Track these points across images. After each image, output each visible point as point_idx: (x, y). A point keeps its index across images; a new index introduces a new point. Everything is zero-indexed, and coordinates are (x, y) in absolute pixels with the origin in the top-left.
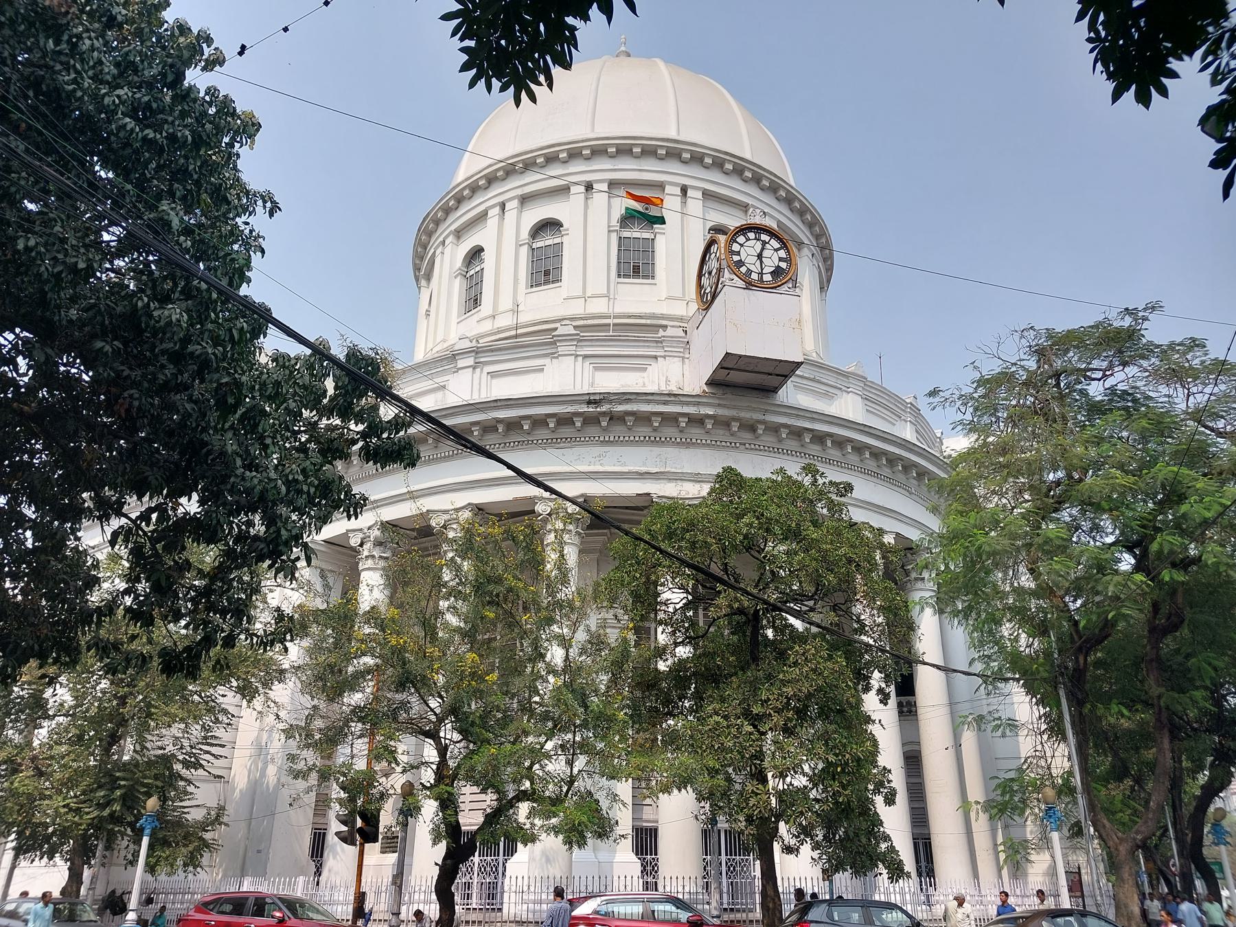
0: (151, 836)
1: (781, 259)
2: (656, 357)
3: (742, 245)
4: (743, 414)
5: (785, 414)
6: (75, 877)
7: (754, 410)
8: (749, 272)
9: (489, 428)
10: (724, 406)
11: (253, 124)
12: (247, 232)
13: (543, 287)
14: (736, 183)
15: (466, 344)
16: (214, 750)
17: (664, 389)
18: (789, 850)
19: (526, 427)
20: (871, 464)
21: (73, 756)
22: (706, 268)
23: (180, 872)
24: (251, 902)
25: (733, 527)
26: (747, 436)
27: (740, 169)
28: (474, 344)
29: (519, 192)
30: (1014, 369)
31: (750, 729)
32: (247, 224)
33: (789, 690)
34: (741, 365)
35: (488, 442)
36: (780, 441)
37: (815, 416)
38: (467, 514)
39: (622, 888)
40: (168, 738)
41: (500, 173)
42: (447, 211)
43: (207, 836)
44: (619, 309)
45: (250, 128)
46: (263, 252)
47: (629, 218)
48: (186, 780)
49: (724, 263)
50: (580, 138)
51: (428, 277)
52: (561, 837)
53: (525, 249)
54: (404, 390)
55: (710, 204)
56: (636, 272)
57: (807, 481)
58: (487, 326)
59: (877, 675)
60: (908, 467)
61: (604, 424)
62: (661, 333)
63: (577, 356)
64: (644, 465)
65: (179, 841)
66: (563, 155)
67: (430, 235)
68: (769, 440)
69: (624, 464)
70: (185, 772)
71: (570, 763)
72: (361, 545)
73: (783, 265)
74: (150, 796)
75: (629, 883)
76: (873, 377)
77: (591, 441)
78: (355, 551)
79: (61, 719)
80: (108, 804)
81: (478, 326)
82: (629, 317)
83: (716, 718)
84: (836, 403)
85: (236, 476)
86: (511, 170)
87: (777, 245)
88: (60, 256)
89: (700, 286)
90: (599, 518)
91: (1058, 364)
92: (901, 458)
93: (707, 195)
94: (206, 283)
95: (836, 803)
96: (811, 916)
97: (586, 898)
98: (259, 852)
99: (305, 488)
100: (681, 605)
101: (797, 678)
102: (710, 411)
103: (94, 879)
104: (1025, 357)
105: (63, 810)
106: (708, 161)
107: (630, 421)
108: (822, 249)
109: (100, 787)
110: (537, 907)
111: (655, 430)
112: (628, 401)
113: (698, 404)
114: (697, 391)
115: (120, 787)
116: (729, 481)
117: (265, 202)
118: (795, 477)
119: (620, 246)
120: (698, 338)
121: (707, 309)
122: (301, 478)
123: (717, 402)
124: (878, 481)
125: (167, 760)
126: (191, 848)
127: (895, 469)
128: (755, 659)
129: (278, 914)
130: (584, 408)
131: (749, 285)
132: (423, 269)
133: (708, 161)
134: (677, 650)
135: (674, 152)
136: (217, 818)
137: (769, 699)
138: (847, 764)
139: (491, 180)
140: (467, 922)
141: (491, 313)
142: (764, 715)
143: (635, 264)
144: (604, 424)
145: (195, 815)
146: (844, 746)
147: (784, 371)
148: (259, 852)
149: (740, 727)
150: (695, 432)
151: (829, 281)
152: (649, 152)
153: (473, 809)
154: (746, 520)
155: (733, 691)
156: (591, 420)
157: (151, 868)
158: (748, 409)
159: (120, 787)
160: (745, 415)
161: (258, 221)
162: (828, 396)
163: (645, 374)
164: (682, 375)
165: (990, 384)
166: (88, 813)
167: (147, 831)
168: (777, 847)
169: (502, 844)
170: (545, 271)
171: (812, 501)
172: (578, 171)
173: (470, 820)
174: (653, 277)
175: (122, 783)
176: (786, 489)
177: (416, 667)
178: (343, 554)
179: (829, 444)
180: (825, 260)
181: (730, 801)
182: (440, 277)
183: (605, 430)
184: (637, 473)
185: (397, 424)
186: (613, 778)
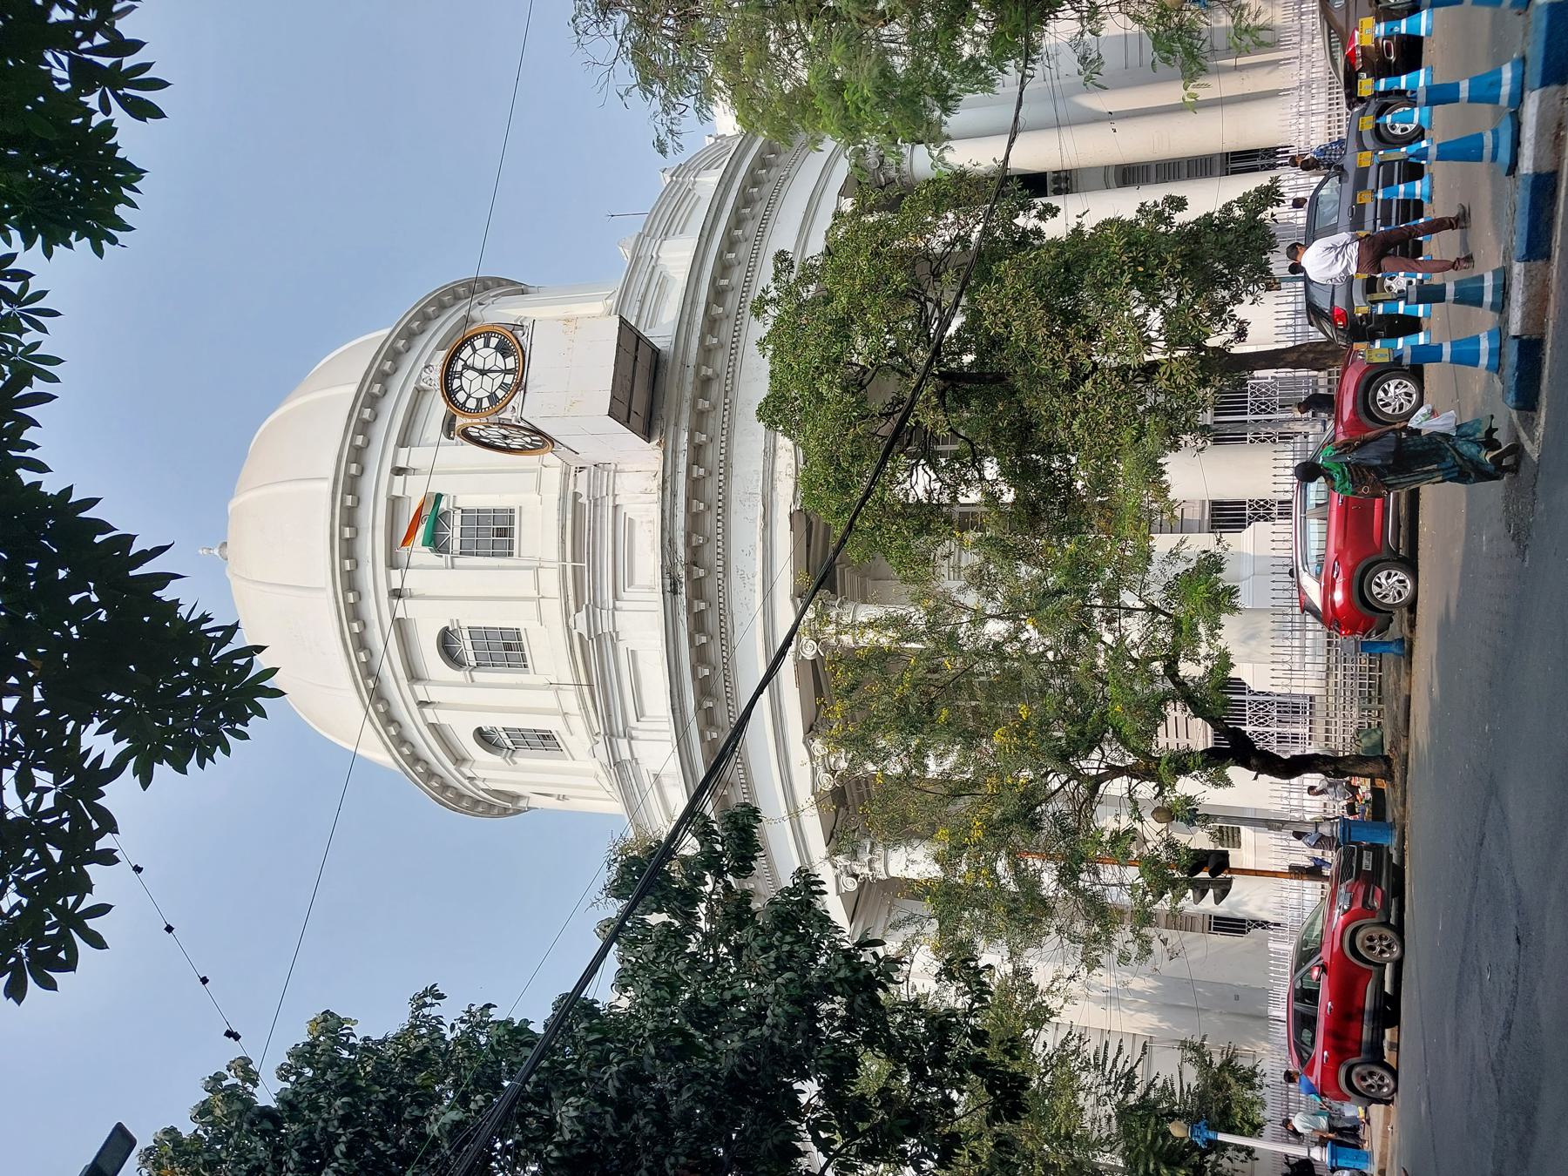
0: (1217, 1131)
1: (487, 345)
2: (615, 507)
3: (469, 396)
4: (688, 394)
5: (687, 340)
7: (682, 380)
8: (503, 386)
9: (708, 719)
11: (325, 1020)
12: (463, 1027)
13: (527, 652)
14: (388, 405)
15: (601, 748)
16: (1112, 1055)
17: (656, 496)
18: (1241, 334)
19: (707, 672)
20: (751, 228)
22: (499, 443)
24: (1299, 1006)
26: (715, 389)
27: (370, 399)
28: (600, 739)
29: (404, 683)
30: (628, 44)
31: (1089, 383)
32: (453, 1027)
33: (1041, 333)
35: (727, 720)
36: (721, 345)
37: (689, 301)
38: (817, 745)
39: (1288, 545)
40: (1095, 1110)
41: (380, 707)
42: (430, 774)
43: (1217, 1061)
44: (554, 554)
45: (330, 1025)
46: (489, 1006)
47: (436, 543)
48: (1149, 1089)
49: (493, 419)
50: (333, 605)
51: (516, 797)
53: (479, 676)
54: (662, 826)
55: (415, 437)
56: (505, 532)
58: (578, 723)
59: (1020, 221)
60: (753, 180)
62: (584, 500)
63: (615, 608)
64: (754, 520)
65: (1223, 1097)
66: (356, 627)
67: (461, 796)
68: (720, 360)
69: (753, 547)
70: (1139, 1091)
71: (1130, 611)
72: (856, 876)
73: (494, 342)
74: (1166, 1134)
75: (1281, 537)
76: (638, 225)
77: (724, 590)
78: (864, 884)
81: (578, 735)
82: (564, 541)
84: (671, 272)
85: (772, 1035)
86: (377, 695)
89: (522, 450)
90: (822, 578)
92: (743, 189)
93: (404, 442)
94: (529, 1076)
95: (1183, 272)
96: (1324, 305)
98: (1237, 998)
99: (786, 948)
101: (1025, 324)
102: (685, 436)
104: (611, 27)
106: (359, 440)
107: (697, 540)
110: (1309, 651)
111: (709, 508)
112: (672, 542)
113: (675, 451)
114: (659, 453)
115: (1157, 1170)
116: (775, 412)
117: (425, 1005)
118: (768, 328)
119: (472, 554)
120: (590, 454)
121: (552, 441)
122: (773, 953)
124: (772, 219)
125: (1124, 1112)
126: (1231, 1081)
128: (1000, 378)
129: (1316, 973)
130: (682, 598)
131: (520, 386)
132: (504, 805)
133: (359, 440)
134: (989, 477)
135: (350, 485)
136: (1196, 1051)
138: (1134, 259)
139: (389, 719)
140: (1327, 739)
141: (560, 718)
142: (1072, 365)
143: (495, 533)
144: (701, 573)
145: (1192, 1076)
146: (1111, 262)
147: (631, 341)
148: (1237, 998)
149: (1087, 397)
150: (712, 455)
151: (513, 283)
152: (349, 517)
153: (1187, 732)
154: (824, 390)
155: (1042, 403)
157: (1256, 1129)
159: (1157, 1170)
160: (688, 392)
163: (637, 521)
164: (637, 472)
165: (648, 75)
167: (1211, 1135)
168: (1238, 349)
170: (506, 649)
171: (800, 305)
172: (377, 610)
173: (1200, 736)
174: (512, 511)
175: (1152, 1166)
176: (783, 341)
177: (1012, 805)
178: (865, 903)
179: (724, 282)
181: (1180, 408)
182: (514, 782)
183: (709, 572)
185: (705, 833)
186: (1149, 558)
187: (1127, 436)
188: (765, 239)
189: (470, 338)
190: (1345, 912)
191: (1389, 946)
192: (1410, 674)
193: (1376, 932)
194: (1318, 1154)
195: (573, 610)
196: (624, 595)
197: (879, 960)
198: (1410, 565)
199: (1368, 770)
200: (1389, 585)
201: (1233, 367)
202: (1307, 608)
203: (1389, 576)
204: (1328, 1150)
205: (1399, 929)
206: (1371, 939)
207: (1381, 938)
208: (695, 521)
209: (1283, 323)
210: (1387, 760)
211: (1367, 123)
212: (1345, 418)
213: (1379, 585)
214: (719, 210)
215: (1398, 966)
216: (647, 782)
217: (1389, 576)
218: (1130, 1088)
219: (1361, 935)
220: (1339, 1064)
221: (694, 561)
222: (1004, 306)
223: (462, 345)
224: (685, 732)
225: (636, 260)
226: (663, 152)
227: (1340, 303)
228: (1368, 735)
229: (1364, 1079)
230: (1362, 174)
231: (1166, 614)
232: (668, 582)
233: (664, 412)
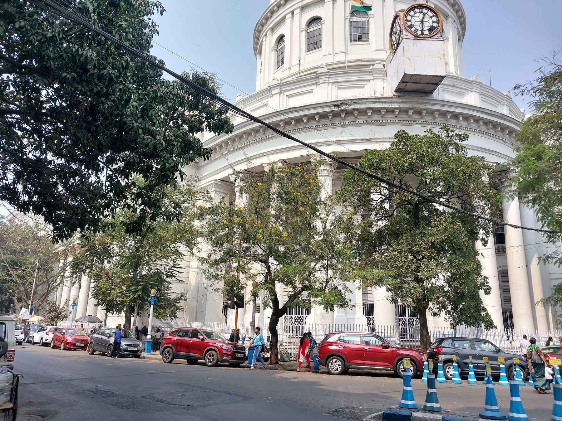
0: (154, 304)
1: (434, 22)
2: (369, 80)
3: (412, 16)
6: (128, 320)
7: (420, 103)
9: (287, 123)
12: (150, 23)
15: (276, 82)
17: (373, 96)
18: (435, 314)
19: (305, 121)
20: (484, 128)
21: (121, 272)
22: (394, 31)
23: (169, 318)
24: (190, 332)
25: (402, 159)
26: (417, 117)
28: (279, 82)
29: (300, 4)
31: (412, 257)
34: (413, 79)
35: (288, 130)
36: (435, 119)
37: (453, 104)
38: (279, 165)
39: (355, 330)
40: (161, 264)
42: (267, 19)
43: (178, 305)
44: (350, 58)
46: (158, 33)
48: (168, 282)
49: (403, 27)
51: (260, 53)
52: (322, 306)
53: (304, 33)
56: (360, 38)
57: (444, 135)
58: (287, 73)
60: (504, 128)
63: (329, 83)
64: (364, 135)
65: (167, 307)
67: (260, 32)
70: (167, 279)
71: (327, 273)
72: (235, 181)
73: (435, 25)
74: (152, 288)
75: (358, 327)
76: (486, 82)
77: (336, 125)
79: (117, 257)
80: (137, 291)
81: (282, 74)
82: (356, 61)
83: (394, 253)
85: (140, 138)
87: (430, 14)
88: (39, 31)
89: (391, 41)
90: (340, 162)
92: (500, 124)
94: (104, 36)
96: (444, 344)
97: (335, 333)
98: (202, 312)
99: (175, 143)
100: (379, 201)
101: (435, 233)
102: (397, 105)
103: (135, 321)
105: (119, 294)
107: (356, 113)
108: (459, 18)
109: (134, 285)
111: (369, 117)
112: (355, 103)
113: (391, 102)
114: (391, 95)
115: (141, 285)
116: (402, 137)
117: (157, 8)
118: (437, 133)
119: (351, 26)
120: (390, 68)
121: (394, 52)
122: (173, 138)
123: (401, 100)
124: (487, 137)
125: (158, 274)
126: (171, 309)
127: (497, 130)
128: (416, 225)
129: (202, 337)
130: (332, 109)
131: (416, 37)
132: (258, 50)
136: (181, 298)
137: (422, 244)
138: (462, 274)
140: (286, 343)
141: (288, 66)
142: (419, 251)
143: (359, 35)
144: (343, 116)
145: (173, 296)
146: (461, 265)
148: (202, 312)
149: (406, 258)
150: (390, 117)
151: (463, 35)
154: (410, 155)
155: (404, 240)
156: (336, 115)
158: (417, 103)
159: (141, 285)
160: (415, 106)
161: (155, 17)
162: (461, 94)
163: (364, 89)
166: (130, 296)
167: (152, 303)
168: (428, 313)
169: (294, 309)
170: (314, 43)
171: (446, 145)
173: (283, 300)
174: (368, 40)
177: (251, 232)
179: (461, 118)
180: (461, 24)
181: (402, 291)
183: (344, 119)
184: (360, 140)
185: (220, 112)
186: (345, 280)
187: (391, 273)
188: (479, 134)
190: (222, 347)
191: (211, 362)
192: (306, 371)
193: (215, 357)
194: (149, 337)
196: (334, 86)
197: (174, 179)
198: (345, 372)
199: (273, 357)
200: (336, 365)
201: (419, 311)
202: (328, 336)
203: (339, 365)
204: (151, 340)
205: (216, 365)
206: (213, 356)
207: (213, 359)
208: (362, 112)
209: (440, 330)
210: (277, 363)
211: (516, 361)
212: (398, 352)
213: (336, 362)
216: (264, 101)
217: (339, 365)
218: (168, 276)
219: (214, 352)
220: (173, 344)
221: (349, 113)
222: (442, 224)
224: (282, 114)
225: (471, 82)
226: (515, 88)
227: (444, 350)
228: (287, 356)
229: (168, 352)
230: (496, 359)
231: (325, 287)
232: (339, 103)
233: (407, 97)
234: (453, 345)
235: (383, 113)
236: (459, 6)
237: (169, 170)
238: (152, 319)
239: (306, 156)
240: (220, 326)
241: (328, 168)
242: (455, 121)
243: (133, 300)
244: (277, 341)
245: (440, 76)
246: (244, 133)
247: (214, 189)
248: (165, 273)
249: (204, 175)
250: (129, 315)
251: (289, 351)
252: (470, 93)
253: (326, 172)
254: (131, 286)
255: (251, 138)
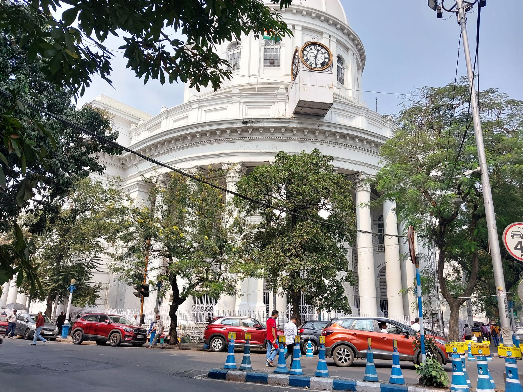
0: (74, 293)
1: (325, 58)
2: (274, 102)
3: (308, 52)
5: (328, 126)
7: (314, 124)
8: (311, 63)
10: (301, 123)
14: (317, 22)
17: (277, 116)
19: (218, 134)
20: (367, 147)
21: (44, 263)
23: (87, 306)
24: (99, 317)
26: (311, 136)
28: (198, 98)
34: (306, 105)
36: (326, 138)
37: (341, 126)
38: (195, 170)
40: (85, 257)
44: (261, 81)
56: (272, 63)
61: (250, 132)
62: (276, 91)
63: (240, 102)
64: (267, 149)
68: (321, 137)
69: (259, 149)
70: (88, 270)
72: (156, 182)
73: (326, 60)
74: (72, 278)
76: (372, 108)
77: (245, 139)
80: (59, 281)
87: (323, 51)
91: (440, 102)
93: (304, 28)
97: (219, 318)
98: (121, 300)
99: (69, 164)
102: (295, 126)
103: (55, 308)
106: (304, 13)
107: (261, 130)
111: (272, 134)
113: (290, 122)
115: (62, 275)
119: (265, 52)
120: (291, 93)
123: (298, 121)
124: (371, 154)
130: (241, 125)
131: (311, 69)
133: (304, 13)
144: (250, 132)
145: (92, 285)
147: (325, 107)
148: (121, 300)
150: (289, 135)
151: (363, 64)
154: (283, 173)
156: (245, 130)
158: (311, 124)
160: (310, 127)
162: (351, 118)
163: (269, 110)
164: (283, 110)
167: (71, 291)
179: (348, 138)
183: (251, 134)
189: (328, 52)
192: (198, 350)
193: (118, 338)
195: (239, 88)
205: (118, 345)
206: (116, 337)
207: (116, 340)
208: (266, 129)
213: (218, 341)
214: (373, 136)
215: (109, 345)
216: (185, 114)
220: (83, 328)
221: (254, 129)
223: (327, 50)
225: (359, 108)
232: (247, 120)
233: (303, 119)
234: (313, 326)
235: (283, 132)
236: (358, 41)
237: (63, 184)
238: (71, 307)
239: (219, 164)
240: (131, 312)
241: (237, 175)
242: (343, 140)
243: (56, 289)
244: (176, 326)
245: (329, 103)
246: (165, 140)
247: (137, 189)
248: (86, 264)
249: (130, 175)
250: (50, 302)
251: (190, 334)
252: (358, 116)
253: (235, 179)
254: (52, 276)
255: (171, 146)
